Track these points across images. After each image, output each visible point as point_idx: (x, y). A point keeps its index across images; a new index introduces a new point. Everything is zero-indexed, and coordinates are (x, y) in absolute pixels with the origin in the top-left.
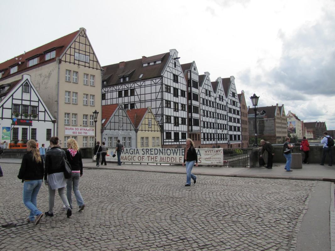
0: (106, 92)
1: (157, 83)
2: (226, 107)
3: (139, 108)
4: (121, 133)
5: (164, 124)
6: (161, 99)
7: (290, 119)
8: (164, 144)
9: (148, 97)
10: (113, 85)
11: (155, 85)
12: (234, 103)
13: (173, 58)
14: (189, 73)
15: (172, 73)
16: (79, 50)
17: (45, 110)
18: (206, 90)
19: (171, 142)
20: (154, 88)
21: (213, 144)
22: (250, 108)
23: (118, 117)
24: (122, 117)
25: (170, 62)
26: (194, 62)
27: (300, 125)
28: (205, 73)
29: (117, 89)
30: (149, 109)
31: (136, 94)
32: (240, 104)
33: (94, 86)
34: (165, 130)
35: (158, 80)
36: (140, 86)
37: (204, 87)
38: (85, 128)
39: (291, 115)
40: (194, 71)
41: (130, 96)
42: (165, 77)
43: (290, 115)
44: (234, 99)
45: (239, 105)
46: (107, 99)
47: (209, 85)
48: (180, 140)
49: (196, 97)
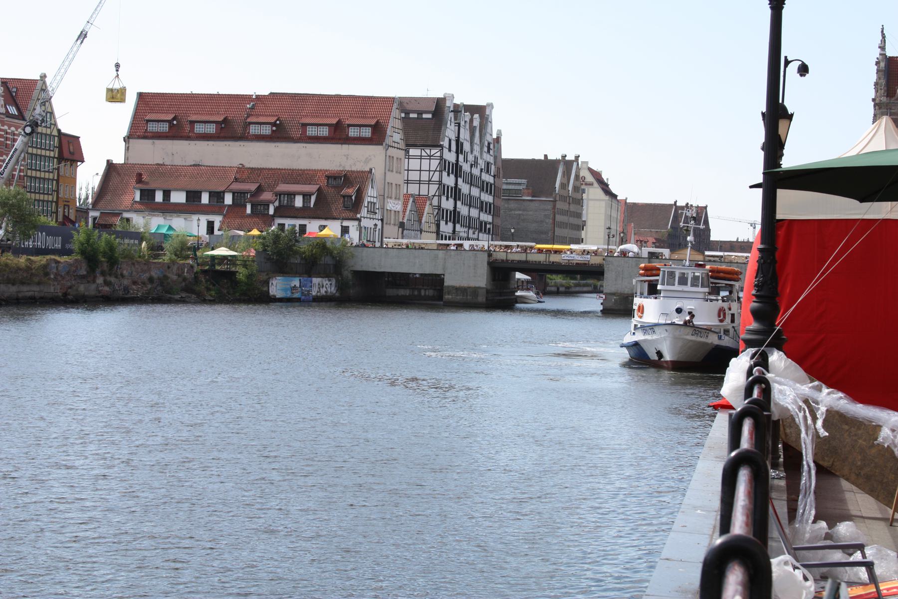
1: (432, 156)
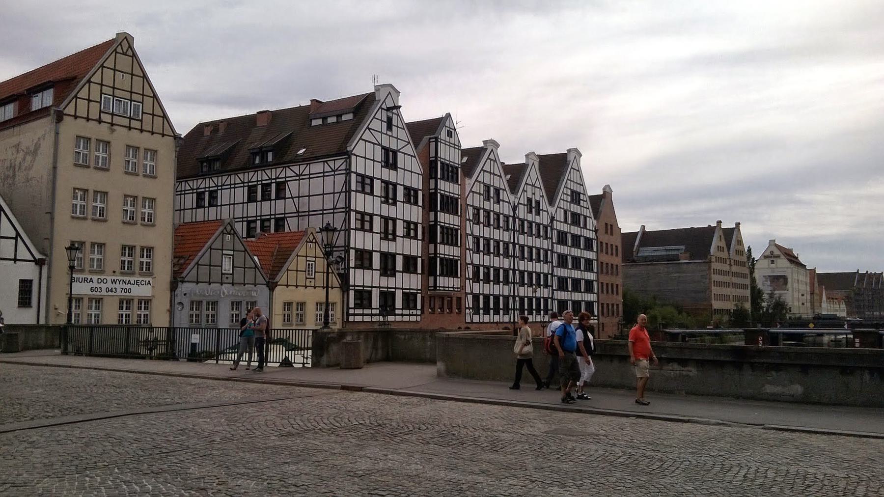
0: (220, 188)
2: (549, 228)
3: (294, 228)
4: (225, 291)
5: (352, 271)
6: (344, 210)
7: (773, 262)
8: (348, 319)
9: (316, 204)
10: (236, 171)
11: (333, 173)
12: (576, 219)
13: (384, 106)
14: (433, 145)
15: (379, 145)
16: (114, 88)
17: (18, 234)
18: (487, 187)
19: (372, 315)
20: (329, 180)
21: (503, 322)
22: (647, 230)
23: (221, 251)
24: (232, 253)
25: (374, 117)
26: (448, 115)
27: (804, 278)
28: (485, 142)
29: (274, 177)
30: (309, 233)
31: (288, 195)
32: (595, 222)
33: (155, 177)
34: (352, 286)
35: (339, 163)
36: (297, 175)
37: (480, 179)
38: (127, 279)
39: (777, 252)
40: (448, 139)
41: (275, 200)
42: (356, 156)
43: (772, 252)
44: (575, 208)
45: (591, 223)
46: (221, 205)
47: (497, 172)
48: (397, 312)
49: (451, 205)
